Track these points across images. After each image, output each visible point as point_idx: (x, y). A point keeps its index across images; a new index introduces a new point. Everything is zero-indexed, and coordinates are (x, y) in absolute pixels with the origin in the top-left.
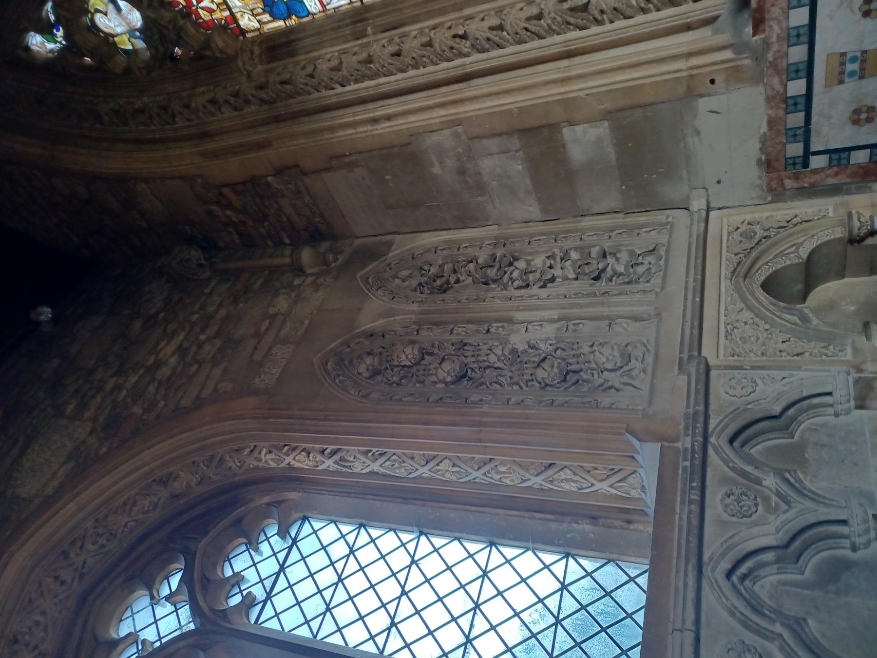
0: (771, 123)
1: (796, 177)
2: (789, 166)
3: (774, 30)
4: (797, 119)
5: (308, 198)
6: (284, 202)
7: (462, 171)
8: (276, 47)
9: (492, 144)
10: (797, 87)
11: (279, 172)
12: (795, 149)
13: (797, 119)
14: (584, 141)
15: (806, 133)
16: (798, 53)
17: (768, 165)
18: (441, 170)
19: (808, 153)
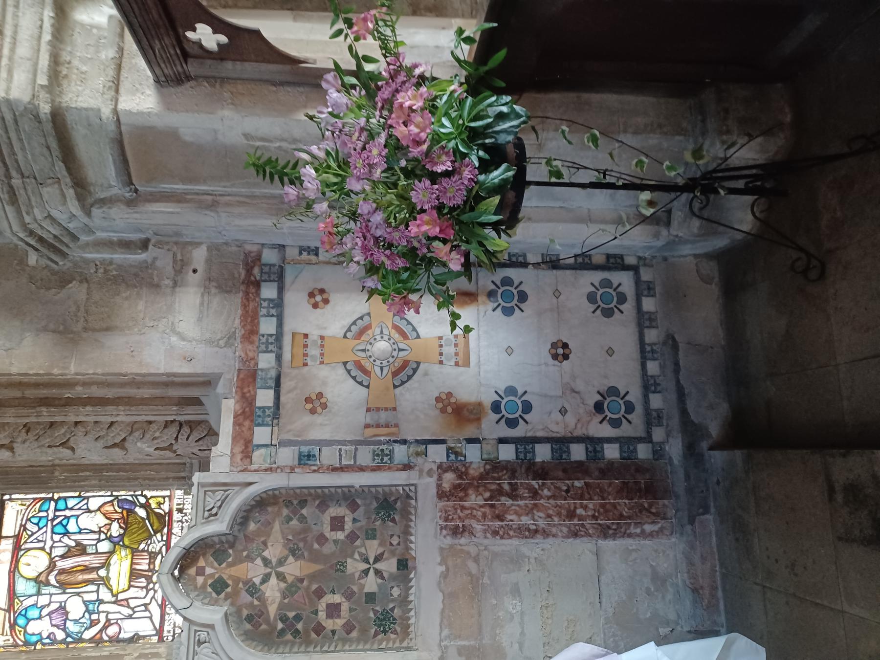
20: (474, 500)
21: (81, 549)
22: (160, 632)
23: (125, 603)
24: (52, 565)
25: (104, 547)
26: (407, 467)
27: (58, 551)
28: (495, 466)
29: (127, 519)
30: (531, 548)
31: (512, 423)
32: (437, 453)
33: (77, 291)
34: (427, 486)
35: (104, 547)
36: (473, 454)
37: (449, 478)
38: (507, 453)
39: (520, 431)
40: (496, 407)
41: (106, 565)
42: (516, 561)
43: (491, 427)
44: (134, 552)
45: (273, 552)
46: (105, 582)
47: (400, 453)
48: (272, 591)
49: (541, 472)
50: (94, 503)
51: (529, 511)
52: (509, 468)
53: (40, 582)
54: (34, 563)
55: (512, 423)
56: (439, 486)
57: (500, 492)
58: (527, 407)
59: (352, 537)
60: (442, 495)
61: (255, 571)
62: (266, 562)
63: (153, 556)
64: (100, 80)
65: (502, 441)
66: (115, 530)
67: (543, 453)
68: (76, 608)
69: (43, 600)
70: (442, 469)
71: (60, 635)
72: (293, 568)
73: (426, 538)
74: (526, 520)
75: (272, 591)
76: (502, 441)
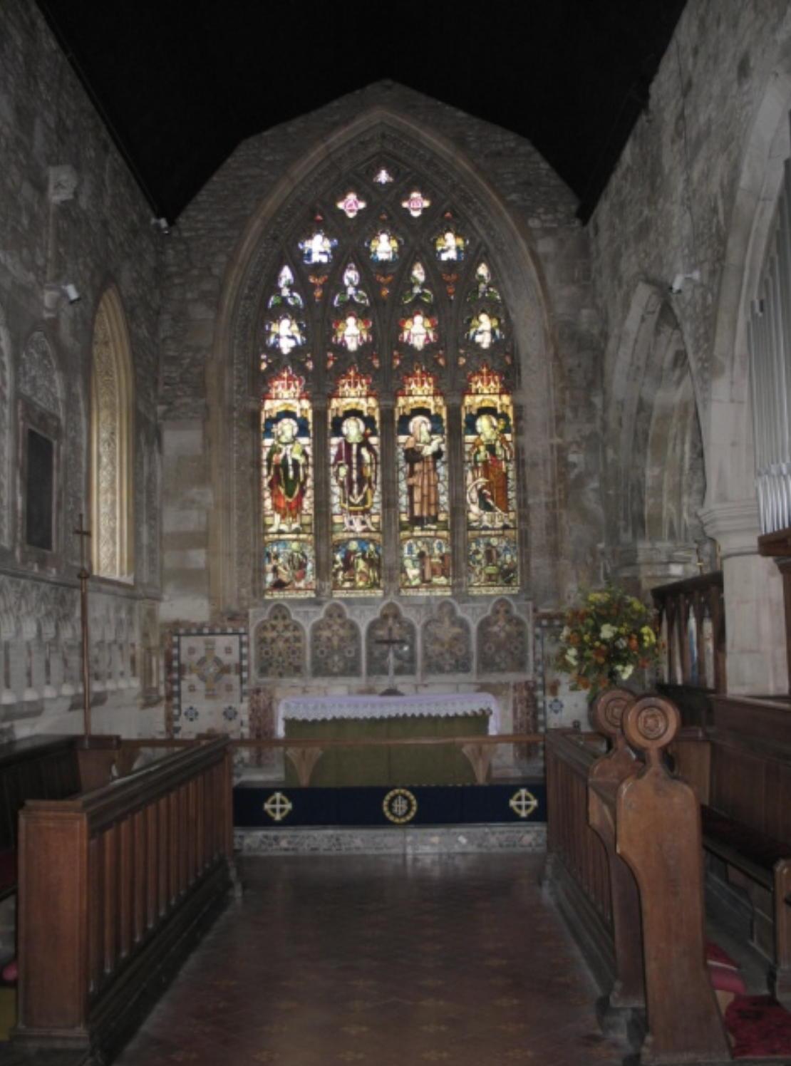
0: (194, 624)
1: (170, 632)
2: (177, 628)
3: (227, 623)
4: (194, 631)
5: (190, 414)
6: (188, 400)
7: (193, 501)
8: (256, 415)
9: (204, 519)
10: (206, 631)
11: (207, 407)
12: (182, 631)
13: (194, 631)
14: (198, 558)
15: (188, 634)
16: (218, 630)
17: (177, 624)
18: (194, 492)
19: (179, 635)
20: (525, 693)
21: (498, 555)
22: (471, 586)
23: (480, 573)
24: (494, 547)
25: (499, 563)
26: (535, 670)
27: (499, 549)
28: (535, 700)
29: (508, 572)
30: (509, 713)
31: (551, 706)
32: (539, 681)
33: (590, 560)
34: (529, 676)
35: (499, 563)
36: (539, 693)
37: (531, 685)
38: (540, 704)
39: (548, 709)
40: (556, 701)
41: (493, 565)
42: (506, 707)
43: (549, 699)
44: (497, 574)
45: (508, 628)
46: (488, 565)
47: (540, 668)
48: (496, 629)
49: (535, 716)
50: (515, 559)
51: (522, 712)
52: (535, 705)
53: (488, 544)
54: (494, 541)
55: (551, 706)
56: (530, 681)
57: (528, 701)
58: (556, 712)
59: (512, 653)
60: (527, 683)
61: (501, 623)
62: (504, 626)
63: (496, 581)
64: (650, 573)
65: (544, 703)
66: (506, 567)
67: (541, 717)
68: (479, 557)
69: (482, 546)
70: (535, 682)
71: (471, 553)
72: (503, 635)
73: (512, 677)
74: (519, 711)
75: (496, 629)
76: (544, 703)
